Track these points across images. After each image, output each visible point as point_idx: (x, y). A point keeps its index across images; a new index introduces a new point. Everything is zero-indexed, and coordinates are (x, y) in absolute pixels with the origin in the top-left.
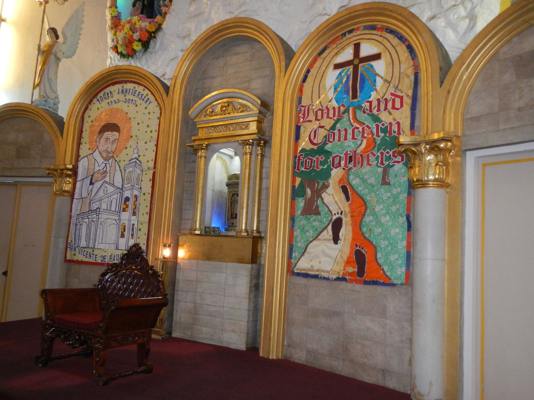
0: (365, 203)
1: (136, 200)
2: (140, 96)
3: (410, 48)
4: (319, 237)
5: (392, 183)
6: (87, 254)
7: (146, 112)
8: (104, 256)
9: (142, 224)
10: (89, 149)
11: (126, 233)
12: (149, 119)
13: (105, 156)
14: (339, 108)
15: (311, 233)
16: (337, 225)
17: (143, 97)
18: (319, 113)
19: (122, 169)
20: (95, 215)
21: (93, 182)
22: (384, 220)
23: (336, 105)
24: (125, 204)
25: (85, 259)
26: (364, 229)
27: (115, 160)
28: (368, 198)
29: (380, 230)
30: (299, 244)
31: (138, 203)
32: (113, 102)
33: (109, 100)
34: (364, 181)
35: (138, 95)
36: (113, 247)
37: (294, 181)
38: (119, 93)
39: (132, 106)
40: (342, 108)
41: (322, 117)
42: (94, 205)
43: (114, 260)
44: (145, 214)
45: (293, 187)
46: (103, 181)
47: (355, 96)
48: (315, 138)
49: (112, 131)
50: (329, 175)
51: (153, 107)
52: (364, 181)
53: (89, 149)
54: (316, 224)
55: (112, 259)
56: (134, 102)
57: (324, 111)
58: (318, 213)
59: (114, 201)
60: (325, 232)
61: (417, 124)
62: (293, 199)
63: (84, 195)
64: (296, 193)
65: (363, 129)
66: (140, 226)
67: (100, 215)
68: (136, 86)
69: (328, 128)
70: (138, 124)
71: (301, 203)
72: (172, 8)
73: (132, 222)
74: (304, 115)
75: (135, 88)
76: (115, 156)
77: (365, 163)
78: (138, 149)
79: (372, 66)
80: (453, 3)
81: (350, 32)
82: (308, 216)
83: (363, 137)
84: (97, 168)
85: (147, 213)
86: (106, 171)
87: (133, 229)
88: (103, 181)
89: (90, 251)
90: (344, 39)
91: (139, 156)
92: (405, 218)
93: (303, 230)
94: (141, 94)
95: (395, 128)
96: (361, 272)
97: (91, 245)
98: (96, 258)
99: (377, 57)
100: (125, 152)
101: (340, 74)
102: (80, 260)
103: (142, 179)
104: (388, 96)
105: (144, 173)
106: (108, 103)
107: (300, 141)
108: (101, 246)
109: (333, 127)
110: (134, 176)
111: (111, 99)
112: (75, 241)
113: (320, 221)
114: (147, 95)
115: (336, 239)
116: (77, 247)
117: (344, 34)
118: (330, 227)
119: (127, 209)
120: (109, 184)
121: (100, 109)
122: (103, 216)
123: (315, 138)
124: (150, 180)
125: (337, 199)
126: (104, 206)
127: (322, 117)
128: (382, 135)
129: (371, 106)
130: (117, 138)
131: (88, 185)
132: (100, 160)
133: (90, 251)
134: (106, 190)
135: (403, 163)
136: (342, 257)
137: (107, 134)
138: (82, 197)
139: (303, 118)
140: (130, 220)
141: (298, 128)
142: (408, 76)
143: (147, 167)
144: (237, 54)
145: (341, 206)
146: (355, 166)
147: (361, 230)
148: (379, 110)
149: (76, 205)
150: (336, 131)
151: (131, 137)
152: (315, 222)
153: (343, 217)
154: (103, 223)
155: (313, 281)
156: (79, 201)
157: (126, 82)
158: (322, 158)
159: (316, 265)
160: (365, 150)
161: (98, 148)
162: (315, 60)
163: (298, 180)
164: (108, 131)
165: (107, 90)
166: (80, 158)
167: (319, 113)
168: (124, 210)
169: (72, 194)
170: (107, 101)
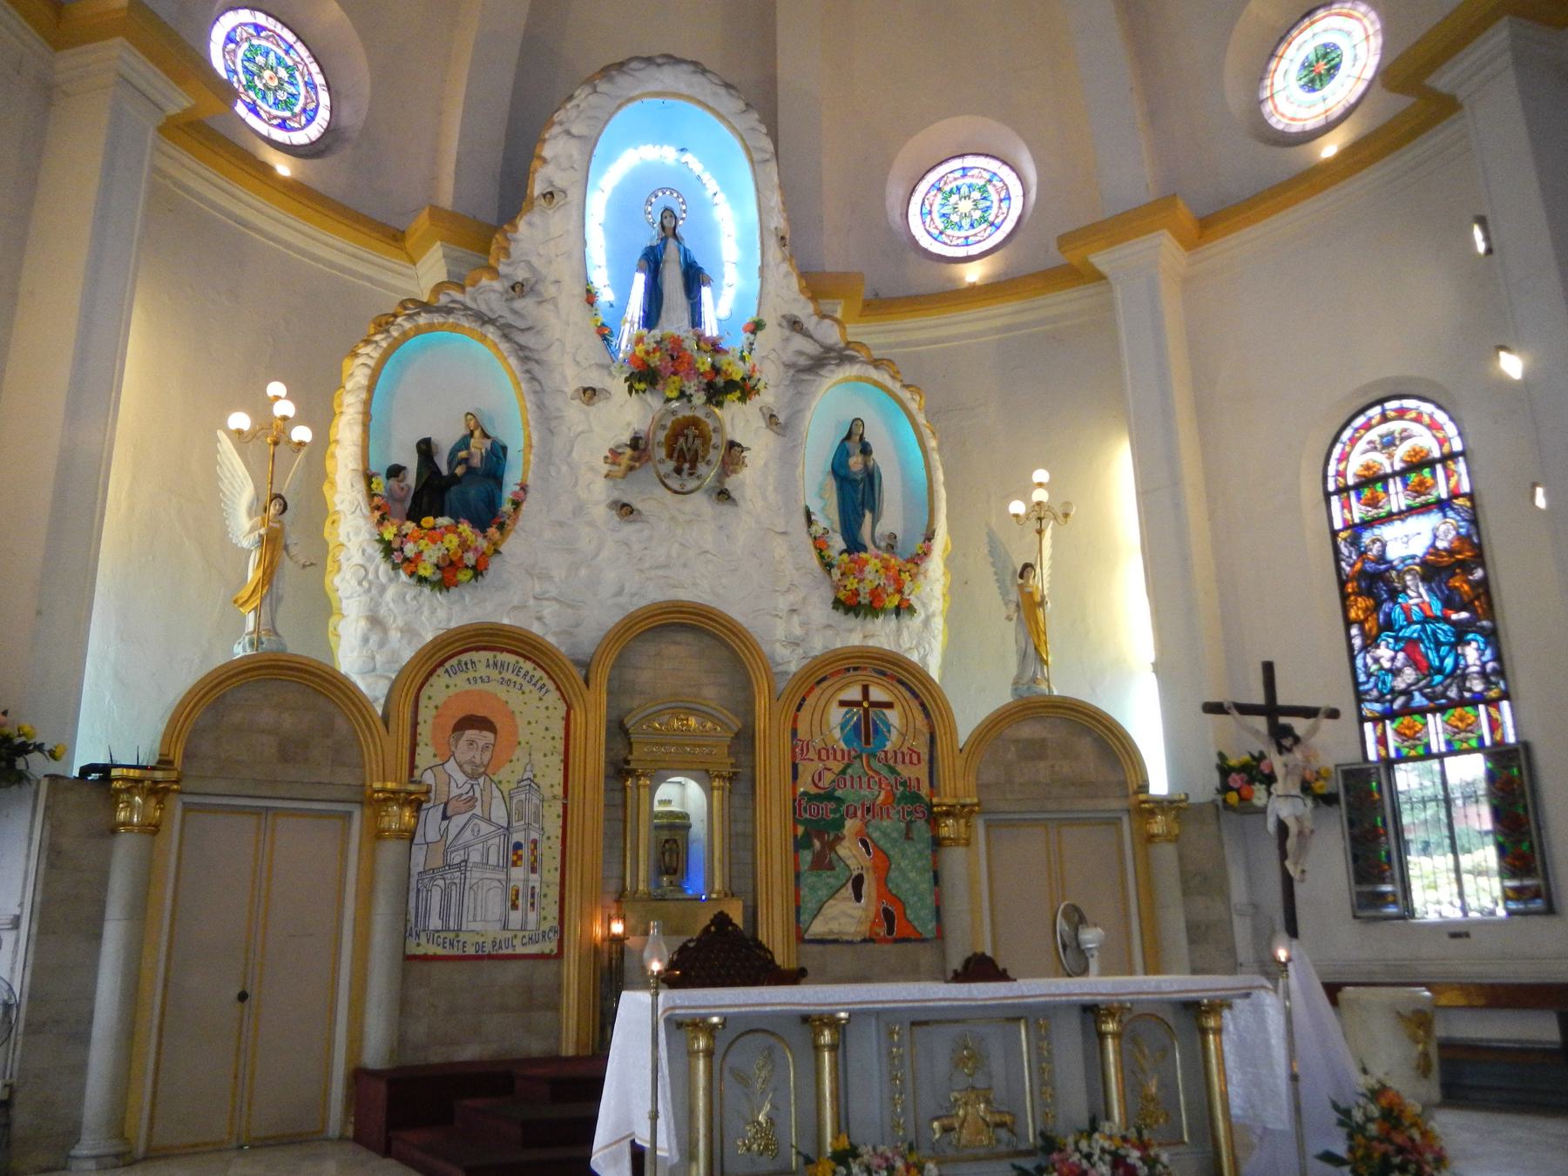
0: (887, 856)
1: (536, 848)
2: (528, 678)
3: (922, 705)
4: (836, 896)
5: (915, 838)
6: (444, 943)
7: (542, 705)
8: (481, 942)
9: (548, 886)
10: (435, 756)
11: (520, 902)
12: (548, 717)
13: (470, 771)
14: (849, 752)
15: (823, 893)
16: (858, 882)
17: (534, 681)
18: (823, 753)
19: (506, 794)
20: (458, 874)
21: (449, 814)
22: (912, 875)
23: (845, 747)
24: (515, 853)
25: (440, 951)
26: (890, 885)
27: (492, 780)
28: (891, 853)
29: (908, 886)
30: (809, 903)
31: (538, 852)
32: (479, 681)
33: (471, 674)
34: (885, 834)
35: (525, 675)
36: (498, 926)
37: (795, 829)
38: (488, 666)
39: (515, 692)
40: (853, 753)
41: (828, 758)
42: (453, 855)
43: (501, 948)
44: (552, 871)
45: (795, 836)
46: (471, 813)
47: (868, 742)
48: (820, 780)
49: (481, 729)
50: (843, 826)
51: (553, 697)
52: (885, 834)
53: (435, 756)
54: (831, 880)
55: (497, 947)
56: (518, 686)
57: (828, 752)
58: (831, 867)
59: (493, 850)
60: (843, 890)
61: (935, 782)
62: (796, 851)
63: (432, 835)
64: (800, 844)
65: (880, 779)
66: (545, 890)
67: (468, 874)
68: (521, 660)
69: (837, 770)
70: (529, 723)
71: (806, 857)
72: (520, 523)
73: (531, 884)
74: (802, 750)
75: (517, 662)
76: (489, 771)
77: (885, 816)
78: (532, 765)
79: (884, 714)
80: (908, 645)
81: (856, 669)
82: (820, 872)
83: (880, 787)
84: (455, 792)
85: (556, 869)
86: (473, 798)
87: (533, 896)
88: (467, 816)
89: (452, 935)
90: (848, 674)
91: (535, 776)
92: (932, 874)
93: (813, 888)
94: (530, 674)
95: (914, 783)
96: (890, 931)
97: (452, 924)
98: (464, 947)
99: (889, 705)
100: (508, 767)
101: (847, 713)
102: (431, 952)
103: (545, 814)
104: (906, 751)
105: (546, 804)
106: (468, 679)
107: (799, 781)
108: (473, 926)
109: (843, 772)
110: (529, 809)
111: (471, 674)
112: (416, 921)
113: (837, 878)
114: (541, 678)
115: (858, 897)
116: (424, 930)
117: (848, 670)
118: (850, 885)
119: (519, 863)
120: (482, 819)
121: (452, 687)
122: (474, 876)
123: (820, 780)
124: (559, 816)
125: (854, 852)
126: (475, 857)
127: (828, 758)
128: (901, 789)
129: (886, 756)
130: (492, 742)
131: (440, 819)
132: (460, 778)
133: (452, 935)
134: (476, 829)
135: (926, 821)
136: (867, 916)
137: (470, 734)
138: (428, 840)
139: (802, 754)
140: (526, 880)
141: (795, 767)
142: (923, 734)
143: (551, 795)
144: (675, 643)
145: (861, 860)
146: (874, 817)
147: (886, 885)
148: (896, 762)
150: (847, 777)
151: (519, 743)
152: (828, 878)
153: (864, 873)
154: (475, 887)
155: (831, 947)
156: (421, 849)
157: (502, 650)
158: (832, 805)
159: (835, 926)
160: (884, 803)
161: (453, 755)
162: (812, 689)
163: (801, 830)
164: (472, 727)
165: (465, 657)
166: (417, 773)
167: (823, 753)
168: (514, 864)
169: (409, 836)
170: (464, 676)
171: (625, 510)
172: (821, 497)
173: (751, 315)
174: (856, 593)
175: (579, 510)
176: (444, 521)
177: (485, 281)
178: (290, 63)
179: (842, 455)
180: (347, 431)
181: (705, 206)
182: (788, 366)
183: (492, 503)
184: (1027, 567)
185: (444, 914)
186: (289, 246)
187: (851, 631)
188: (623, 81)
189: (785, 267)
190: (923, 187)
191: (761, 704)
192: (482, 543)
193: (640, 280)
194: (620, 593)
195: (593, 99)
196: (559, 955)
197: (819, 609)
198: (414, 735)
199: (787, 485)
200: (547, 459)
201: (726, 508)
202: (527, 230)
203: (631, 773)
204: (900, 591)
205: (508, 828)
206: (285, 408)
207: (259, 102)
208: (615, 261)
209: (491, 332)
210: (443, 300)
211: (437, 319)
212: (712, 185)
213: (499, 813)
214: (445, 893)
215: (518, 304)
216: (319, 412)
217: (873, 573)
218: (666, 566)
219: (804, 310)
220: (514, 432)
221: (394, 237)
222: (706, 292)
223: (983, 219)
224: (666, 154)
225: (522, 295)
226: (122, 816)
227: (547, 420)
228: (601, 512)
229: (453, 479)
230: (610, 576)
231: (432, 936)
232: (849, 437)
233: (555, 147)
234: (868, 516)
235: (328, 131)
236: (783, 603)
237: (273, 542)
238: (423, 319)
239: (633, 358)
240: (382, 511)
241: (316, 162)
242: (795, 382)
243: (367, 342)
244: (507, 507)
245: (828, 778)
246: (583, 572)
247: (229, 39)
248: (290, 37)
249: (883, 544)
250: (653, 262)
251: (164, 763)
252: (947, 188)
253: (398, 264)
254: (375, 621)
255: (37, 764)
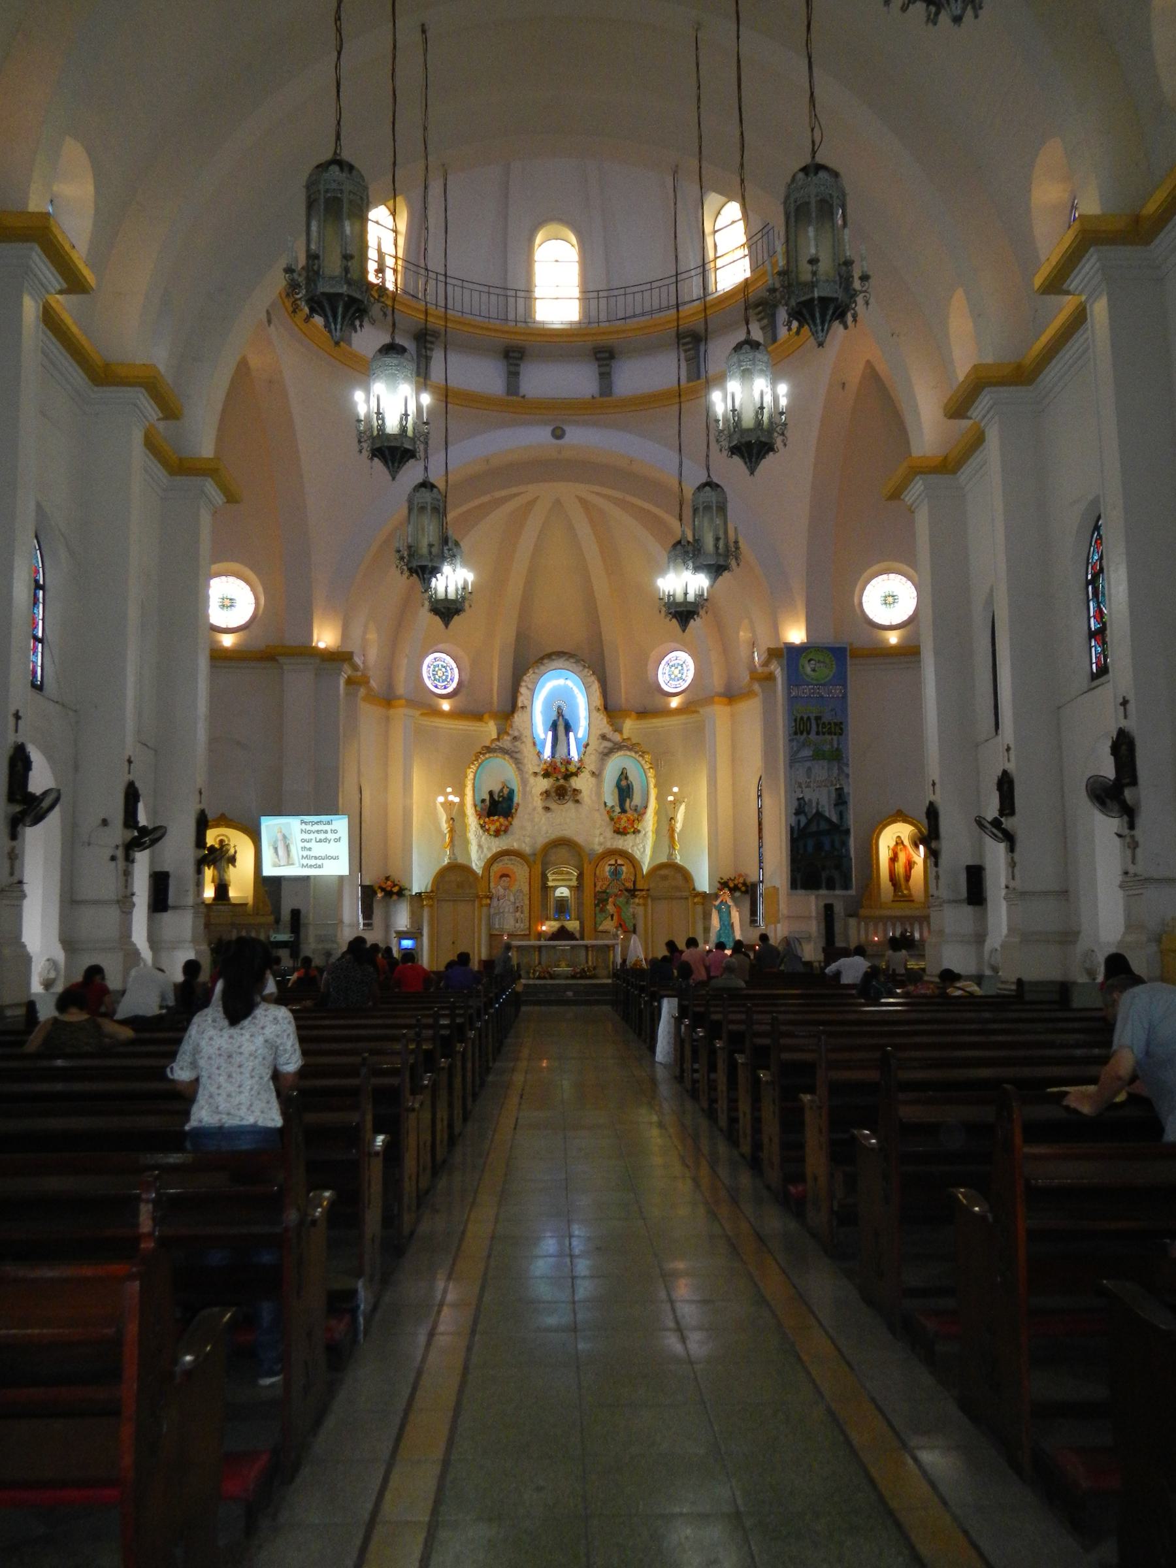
16: (612, 916)
30: (598, 923)
51: (526, 867)
64: (596, 905)
71: (598, 908)
99: (623, 865)
111: (503, 862)
115: (612, 920)
122: (506, 915)
126: (506, 910)
137: (504, 878)
149: (492, 911)
158: (605, 894)
169: (489, 905)
171: (547, 809)
172: (613, 795)
173: (584, 742)
174: (619, 828)
175: (534, 809)
176: (496, 818)
177: (505, 737)
178: (445, 665)
179: (619, 780)
180: (469, 791)
181: (574, 697)
182: (600, 753)
183: (510, 807)
184: (672, 818)
185: (499, 924)
186: (450, 729)
187: (619, 839)
188: (542, 668)
189: (602, 716)
190: (664, 662)
191: (585, 866)
192: (506, 823)
193: (550, 734)
194: (547, 833)
195: (533, 676)
196: (529, 935)
197: (609, 833)
198: (489, 880)
199: (599, 793)
200: (524, 793)
201: (577, 805)
202: (518, 718)
203: (548, 887)
204: (633, 827)
205: (515, 903)
206: (451, 798)
207: (438, 684)
208: (544, 723)
209: (507, 757)
210: (494, 745)
211: (491, 755)
212: (576, 690)
213: (512, 899)
214: (500, 919)
215: (516, 743)
216: (461, 793)
217: (623, 823)
218: (560, 825)
219: (607, 729)
220: (516, 785)
221: (478, 716)
222: (571, 734)
223: (681, 678)
224: (561, 682)
225: (517, 741)
226: (425, 903)
227: (524, 782)
228: (540, 810)
229: (499, 802)
230: (544, 828)
231: (496, 930)
232: (622, 773)
233: (523, 690)
234: (628, 800)
235: (459, 684)
236: (598, 832)
237: (452, 831)
238: (487, 756)
239: (543, 770)
240: (480, 816)
241: (456, 698)
242: (602, 760)
243: (473, 764)
244: (513, 811)
245: (605, 887)
246: (536, 828)
247: (429, 667)
248: (443, 656)
249: (633, 808)
250: (554, 727)
251: (432, 891)
252: (671, 664)
253: (484, 725)
254: (480, 846)
255: (407, 893)
